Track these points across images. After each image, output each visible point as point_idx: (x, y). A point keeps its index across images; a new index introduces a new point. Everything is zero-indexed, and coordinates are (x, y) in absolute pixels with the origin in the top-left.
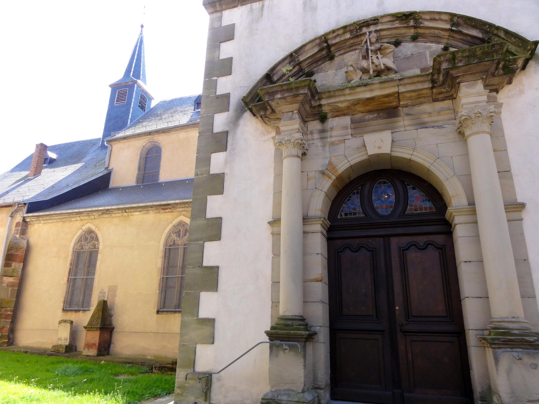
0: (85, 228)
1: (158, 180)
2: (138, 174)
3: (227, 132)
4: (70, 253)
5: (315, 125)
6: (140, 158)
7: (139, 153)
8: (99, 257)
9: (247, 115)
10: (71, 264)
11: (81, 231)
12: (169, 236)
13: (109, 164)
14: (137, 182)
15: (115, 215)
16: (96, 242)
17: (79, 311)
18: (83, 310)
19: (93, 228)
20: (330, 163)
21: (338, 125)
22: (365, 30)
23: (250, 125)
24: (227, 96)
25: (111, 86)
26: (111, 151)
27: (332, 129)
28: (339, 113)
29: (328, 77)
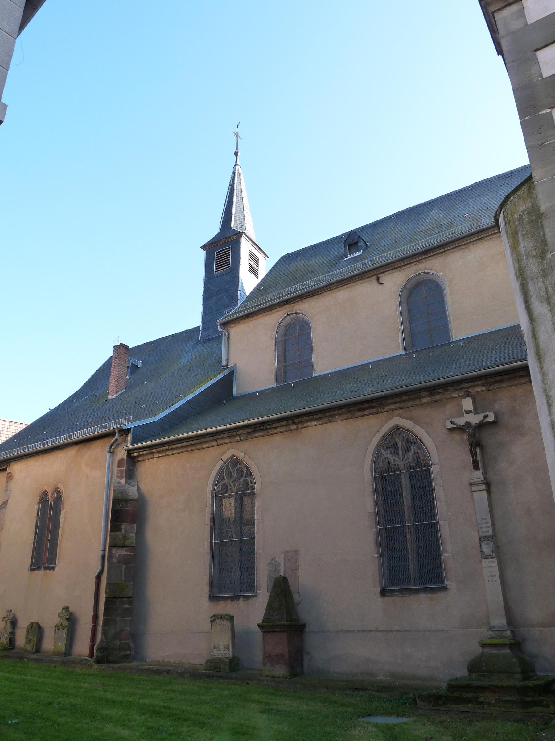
0: (225, 457)
2: (278, 368)
4: (209, 501)
6: (277, 342)
10: (212, 520)
11: (221, 463)
12: (377, 456)
13: (228, 359)
14: (278, 381)
15: (275, 431)
16: (249, 479)
17: (237, 598)
18: (244, 597)
19: (240, 455)
25: (203, 247)
26: (228, 339)
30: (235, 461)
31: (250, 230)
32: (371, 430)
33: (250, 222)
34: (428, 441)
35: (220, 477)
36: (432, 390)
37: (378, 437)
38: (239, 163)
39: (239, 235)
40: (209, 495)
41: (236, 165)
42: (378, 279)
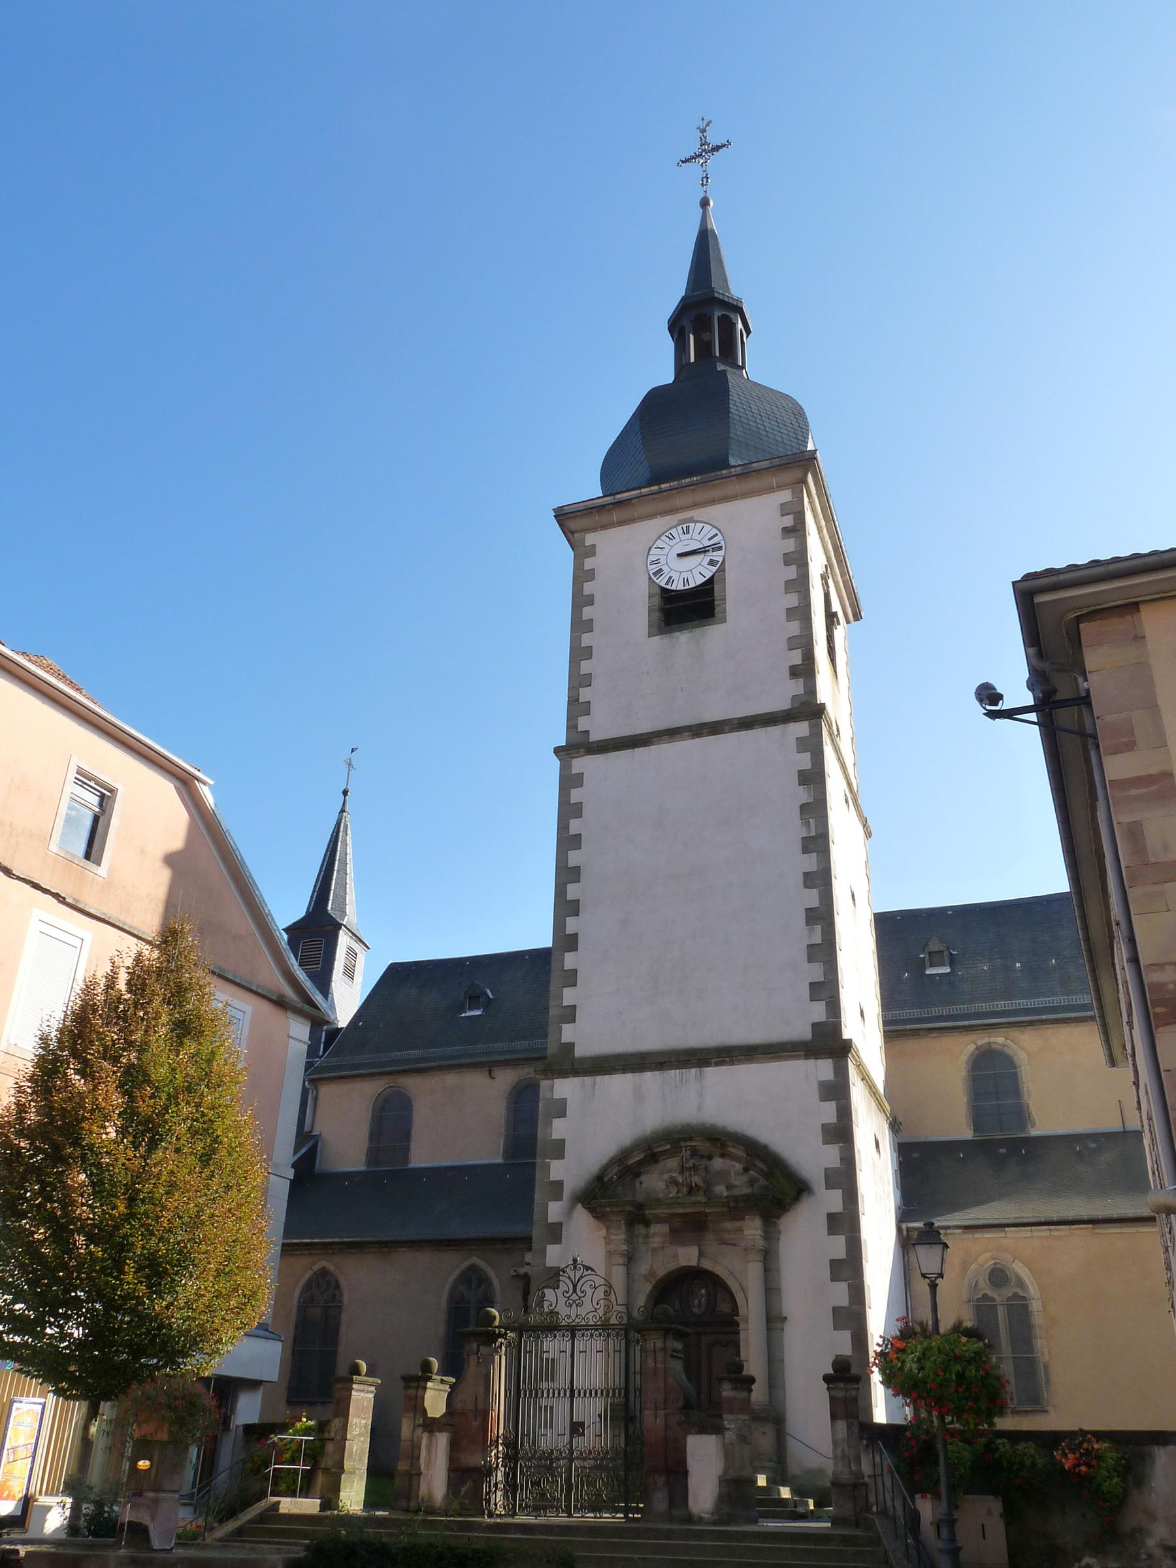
0: (316, 1267)
3: (561, 1224)
4: (295, 1310)
5: (641, 1229)
7: (370, 1108)
8: (344, 1317)
9: (579, 1206)
11: (310, 1273)
12: (454, 1289)
13: (313, 1125)
17: (315, 1403)
19: (330, 1267)
20: (651, 1268)
22: (683, 1144)
23: (582, 1217)
24: (559, 1184)
27: (654, 1235)
28: (660, 1220)
29: (654, 1182)
30: (324, 1272)
31: (351, 917)
32: (452, 1266)
33: (353, 907)
34: (496, 1282)
35: (308, 1287)
36: (504, 1241)
37: (457, 1272)
38: (347, 808)
39: (339, 926)
40: (295, 1302)
41: (343, 811)
42: (490, 1071)
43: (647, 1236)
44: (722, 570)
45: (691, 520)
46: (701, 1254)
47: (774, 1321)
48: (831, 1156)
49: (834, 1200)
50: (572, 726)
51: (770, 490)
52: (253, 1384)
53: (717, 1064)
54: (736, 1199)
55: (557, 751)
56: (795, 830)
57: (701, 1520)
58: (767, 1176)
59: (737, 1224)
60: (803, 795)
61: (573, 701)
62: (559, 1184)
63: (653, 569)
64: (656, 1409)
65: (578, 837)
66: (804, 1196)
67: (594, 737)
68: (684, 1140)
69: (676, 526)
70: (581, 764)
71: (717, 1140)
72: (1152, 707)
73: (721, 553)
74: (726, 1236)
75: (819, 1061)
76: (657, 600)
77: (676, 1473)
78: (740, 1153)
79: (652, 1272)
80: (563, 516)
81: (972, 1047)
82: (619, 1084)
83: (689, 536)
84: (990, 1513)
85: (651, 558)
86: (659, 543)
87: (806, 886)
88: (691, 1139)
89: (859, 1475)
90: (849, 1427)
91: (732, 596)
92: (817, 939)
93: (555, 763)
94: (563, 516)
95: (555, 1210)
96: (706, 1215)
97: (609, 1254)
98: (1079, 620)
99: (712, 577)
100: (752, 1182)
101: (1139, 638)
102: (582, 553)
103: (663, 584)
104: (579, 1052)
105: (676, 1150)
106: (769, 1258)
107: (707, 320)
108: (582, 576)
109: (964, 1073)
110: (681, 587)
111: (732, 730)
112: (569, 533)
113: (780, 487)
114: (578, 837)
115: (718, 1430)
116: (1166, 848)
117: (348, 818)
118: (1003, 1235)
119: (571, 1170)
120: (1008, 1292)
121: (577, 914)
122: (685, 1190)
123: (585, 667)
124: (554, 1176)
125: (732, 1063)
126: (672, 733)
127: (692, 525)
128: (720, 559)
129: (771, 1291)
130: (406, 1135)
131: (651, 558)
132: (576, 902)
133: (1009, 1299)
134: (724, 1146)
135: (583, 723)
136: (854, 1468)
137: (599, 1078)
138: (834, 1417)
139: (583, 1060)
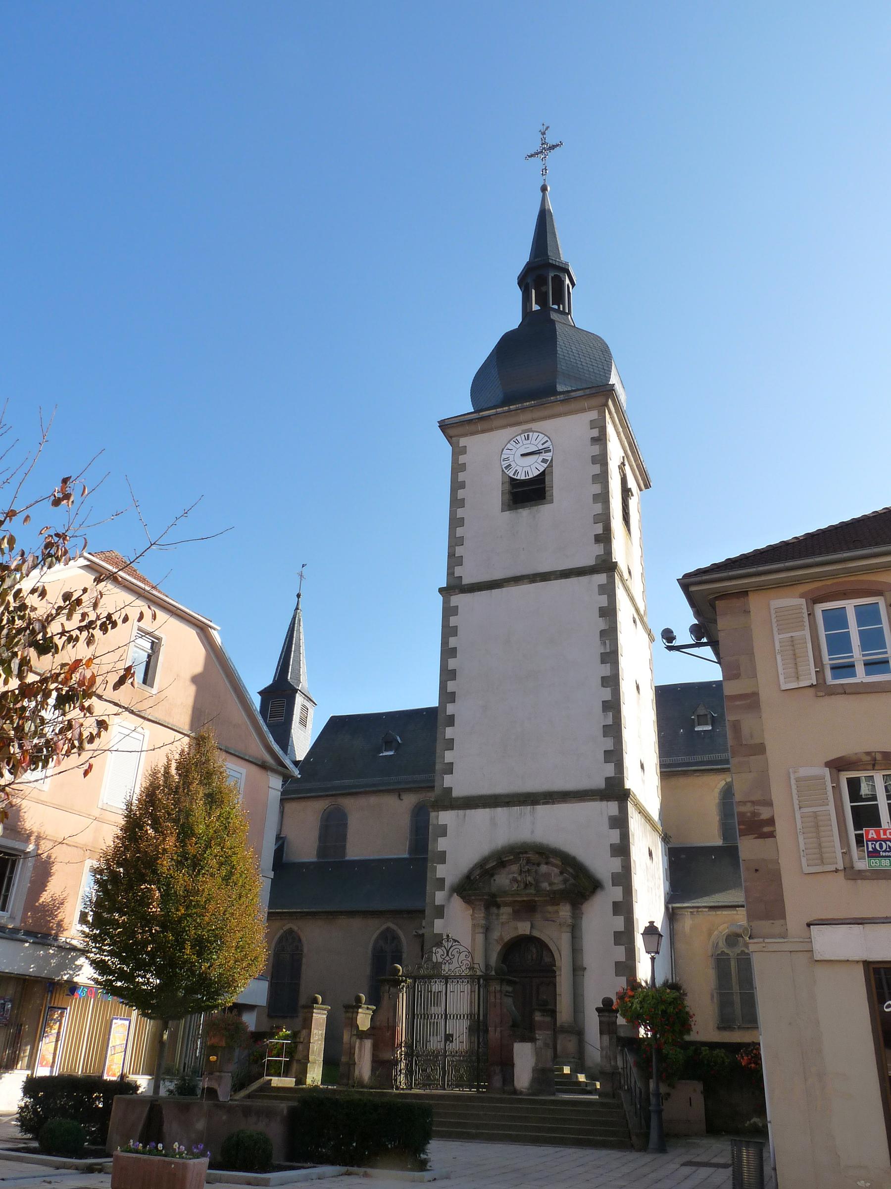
0: (285, 928)
1: (344, 854)
5: (494, 910)
17: (285, 1017)
19: (295, 928)
20: (501, 935)
21: (506, 912)
23: (457, 901)
24: (442, 880)
28: (506, 904)
29: (503, 880)
30: (290, 932)
31: (304, 684)
32: (374, 929)
33: (305, 678)
35: (280, 940)
36: (409, 912)
37: (378, 932)
38: (300, 607)
39: (296, 691)
41: (297, 609)
42: (399, 795)
43: (498, 915)
44: (550, 466)
45: (530, 430)
46: (532, 927)
47: (578, 970)
48: (616, 864)
49: (617, 893)
50: (450, 573)
51: (583, 410)
52: (250, 1008)
53: (544, 804)
54: (554, 892)
55: (441, 590)
56: (597, 648)
57: (521, 1093)
58: (576, 877)
59: (556, 908)
60: (602, 624)
61: (451, 555)
62: (442, 880)
63: (505, 464)
64: (496, 1027)
65: (454, 650)
66: (599, 890)
67: (466, 581)
68: (522, 853)
69: (520, 434)
70: (457, 600)
71: (543, 853)
72: (751, 654)
73: (550, 454)
74: (549, 916)
75: (609, 803)
76: (507, 487)
77: (507, 1064)
78: (559, 863)
79: (501, 938)
80: (444, 426)
81: (723, 783)
82: (481, 815)
83: (528, 442)
84: (695, 1091)
85: (504, 456)
86: (509, 446)
87: (603, 686)
88: (526, 853)
89: (616, 1067)
90: (610, 1040)
91: (557, 485)
92: (610, 721)
93: (438, 600)
94: (444, 426)
95: (440, 897)
96: (535, 902)
97: (474, 926)
98: (716, 598)
99: (544, 471)
100: (565, 881)
101: (747, 612)
102: (458, 451)
103: (511, 475)
104: (455, 794)
105: (517, 859)
106: (575, 930)
107: (544, 278)
108: (457, 468)
109: (717, 801)
110: (523, 478)
111: (556, 579)
112: (449, 438)
113: (590, 409)
114: (454, 650)
115: (532, 1040)
116: (752, 736)
117: (301, 614)
118: (735, 912)
119: (449, 871)
120: (738, 950)
121: (454, 702)
122: (522, 885)
123: (460, 532)
124: (439, 875)
125: (553, 803)
126: (517, 580)
127: (531, 434)
128: (550, 459)
129: (576, 950)
130: (343, 837)
131: (504, 456)
132: (453, 693)
133: (738, 955)
134: (547, 858)
135: (458, 572)
136: (613, 1063)
137: (468, 812)
138: (601, 1033)
139: (458, 799)
